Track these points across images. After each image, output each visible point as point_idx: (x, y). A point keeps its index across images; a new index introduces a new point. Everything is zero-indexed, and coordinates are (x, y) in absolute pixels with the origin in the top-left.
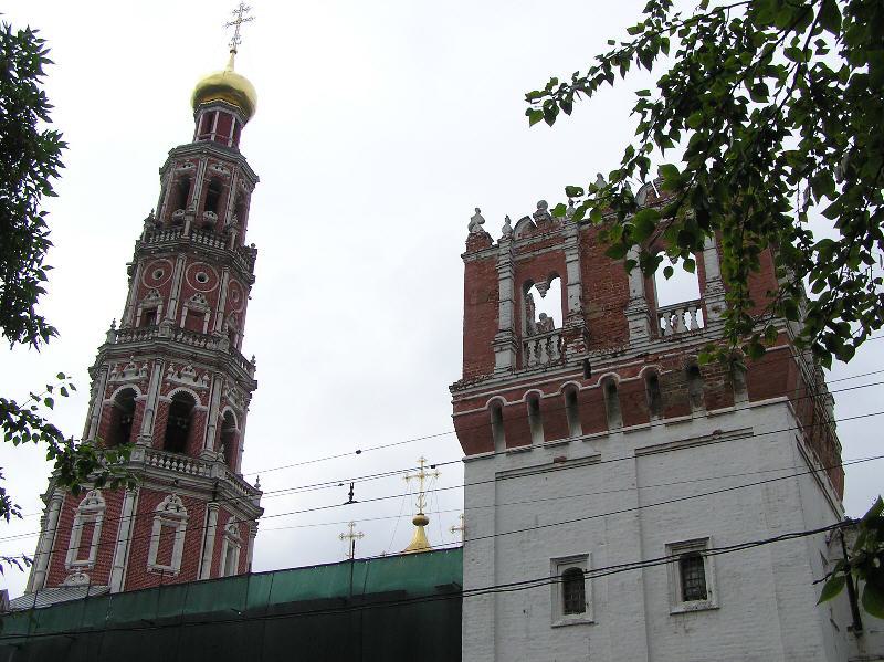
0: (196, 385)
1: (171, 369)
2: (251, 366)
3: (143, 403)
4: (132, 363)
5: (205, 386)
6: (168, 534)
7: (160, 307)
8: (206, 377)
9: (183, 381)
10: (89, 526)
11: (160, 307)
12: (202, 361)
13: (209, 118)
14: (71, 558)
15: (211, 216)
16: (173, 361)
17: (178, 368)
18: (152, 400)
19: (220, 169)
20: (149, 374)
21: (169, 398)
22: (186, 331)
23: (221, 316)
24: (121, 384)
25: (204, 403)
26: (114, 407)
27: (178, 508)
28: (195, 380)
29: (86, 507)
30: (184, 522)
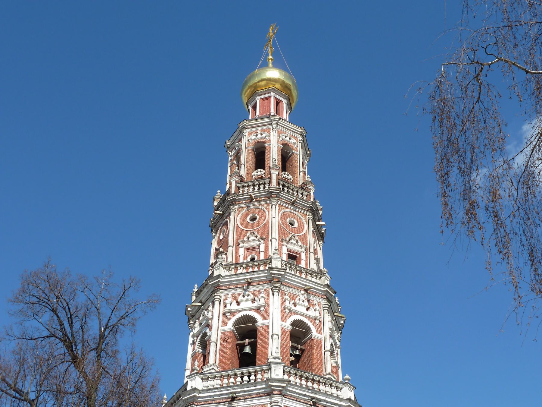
1: (287, 297)
3: (266, 328)
7: (262, 248)
8: (317, 307)
11: (262, 248)
19: (288, 138)
20: (267, 301)
24: (240, 311)
25: (319, 331)
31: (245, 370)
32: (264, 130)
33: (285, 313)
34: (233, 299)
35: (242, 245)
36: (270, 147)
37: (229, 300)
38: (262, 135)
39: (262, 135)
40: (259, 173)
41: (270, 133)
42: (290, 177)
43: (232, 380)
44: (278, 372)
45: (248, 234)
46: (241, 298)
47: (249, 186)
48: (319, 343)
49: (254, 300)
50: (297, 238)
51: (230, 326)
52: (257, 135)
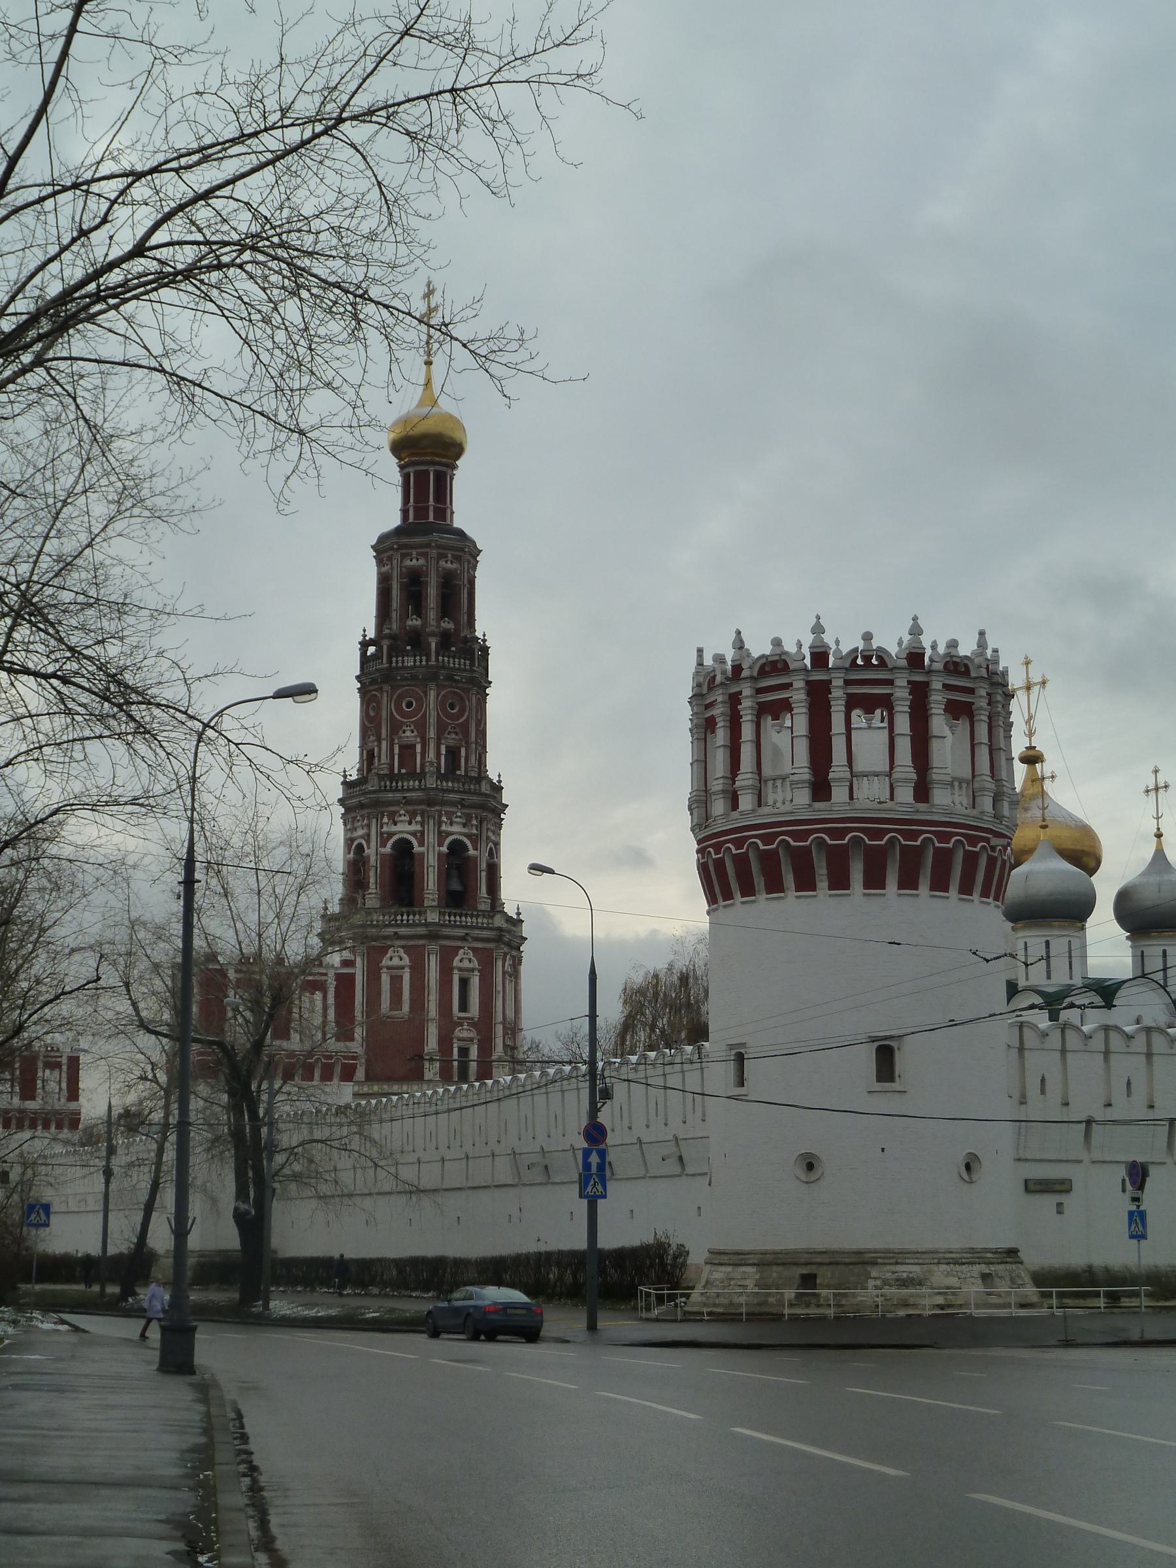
0: (466, 830)
1: (444, 819)
2: (497, 788)
4: (402, 812)
6: (464, 983)
7: (418, 748)
8: (474, 822)
9: (456, 828)
10: (396, 981)
11: (418, 748)
12: (470, 807)
13: (422, 478)
15: (448, 625)
17: (449, 815)
18: (431, 854)
21: (444, 849)
26: (391, 855)
27: (470, 960)
28: (464, 825)
29: (390, 963)
30: (476, 973)
31: (404, 910)
33: (442, 836)
34: (389, 820)
35: (396, 741)
37: (385, 820)
40: (415, 622)
42: (451, 626)
44: (433, 917)
45: (405, 728)
51: (388, 849)
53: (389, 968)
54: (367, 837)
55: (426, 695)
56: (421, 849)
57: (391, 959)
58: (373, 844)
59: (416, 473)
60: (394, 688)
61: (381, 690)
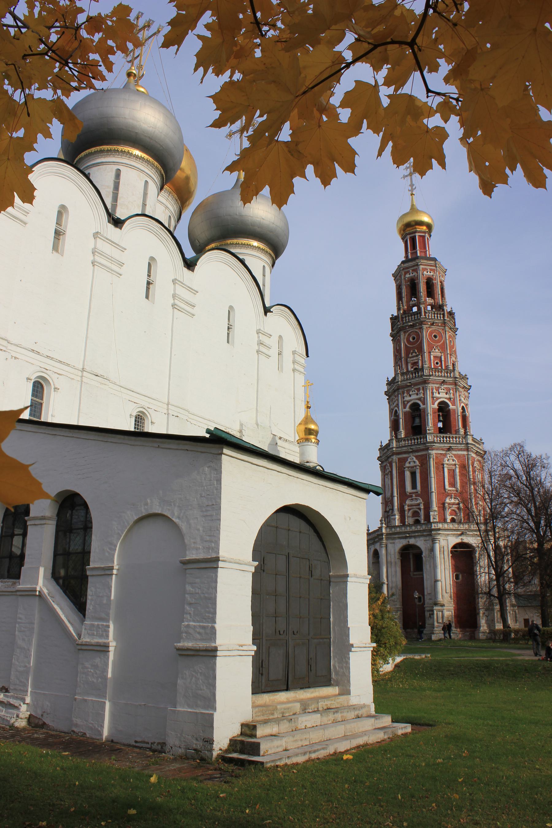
0: (447, 396)
3: (424, 409)
5: (452, 396)
9: (441, 395)
14: (409, 488)
16: (434, 386)
17: (438, 389)
19: (429, 272)
22: (436, 370)
23: (449, 355)
28: (446, 394)
32: (413, 270)
36: (418, 282)
37: (405, 395)
38: (413, 274)
39: (413, 274)
41: (417, 273)
43: (410, 442)
46: (411, 393)
47: (409, 316)
48: (454, 410)
49: (417, 394)
50: (439, 348)
51: (407, 409)
52: (410, 274)
53: (408, 467)
54: (397, 405)
55: (421, 332)
56: (424, 406)
57: (410, 463)
58: (400, 408)
59: (410, 237)
60: (405, 332)
61: (400, 336)
